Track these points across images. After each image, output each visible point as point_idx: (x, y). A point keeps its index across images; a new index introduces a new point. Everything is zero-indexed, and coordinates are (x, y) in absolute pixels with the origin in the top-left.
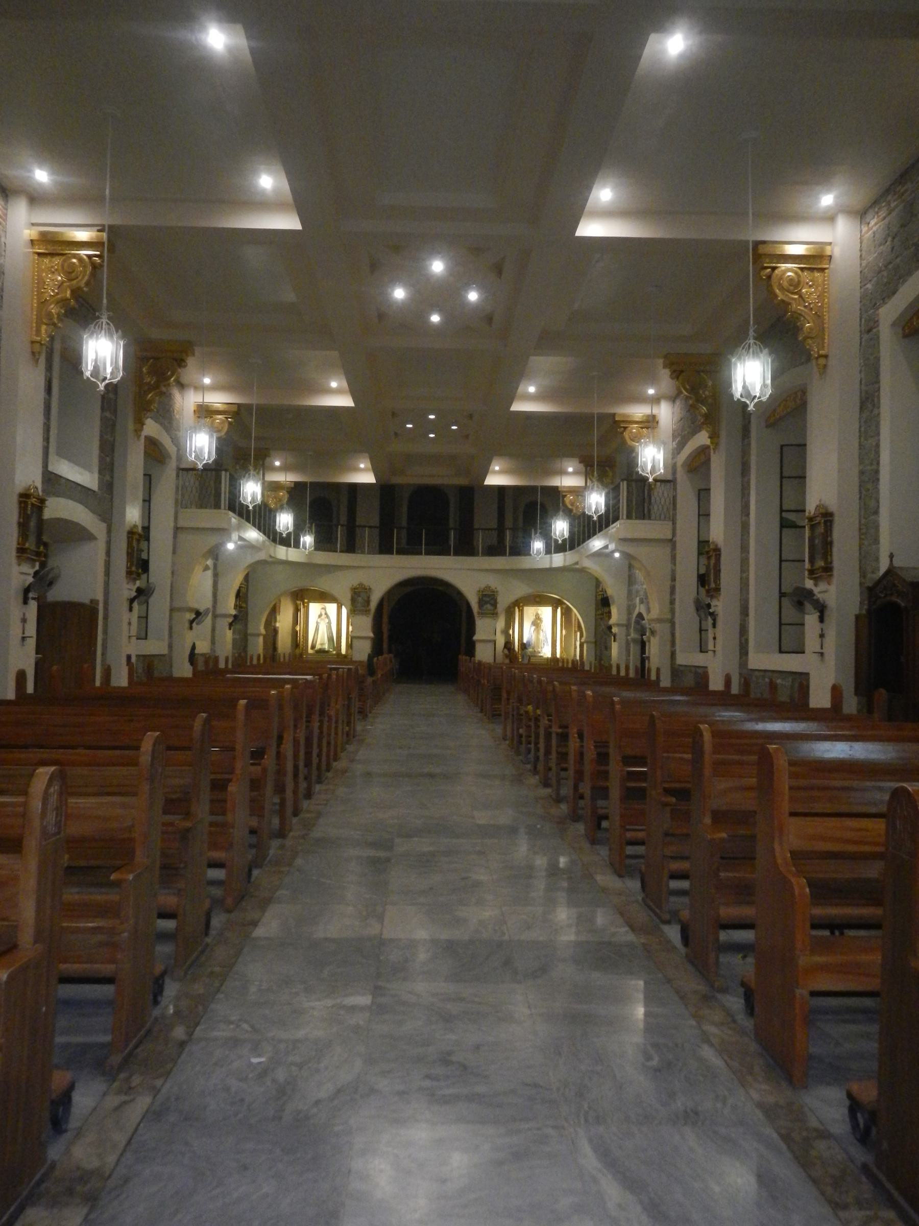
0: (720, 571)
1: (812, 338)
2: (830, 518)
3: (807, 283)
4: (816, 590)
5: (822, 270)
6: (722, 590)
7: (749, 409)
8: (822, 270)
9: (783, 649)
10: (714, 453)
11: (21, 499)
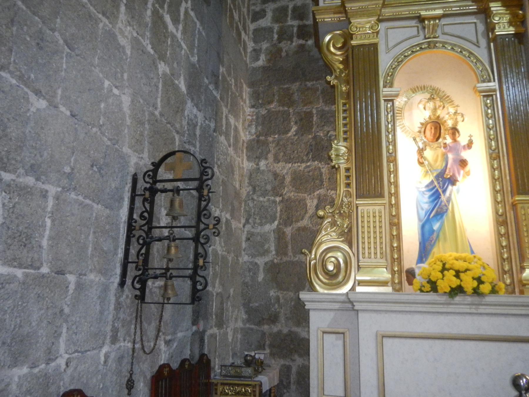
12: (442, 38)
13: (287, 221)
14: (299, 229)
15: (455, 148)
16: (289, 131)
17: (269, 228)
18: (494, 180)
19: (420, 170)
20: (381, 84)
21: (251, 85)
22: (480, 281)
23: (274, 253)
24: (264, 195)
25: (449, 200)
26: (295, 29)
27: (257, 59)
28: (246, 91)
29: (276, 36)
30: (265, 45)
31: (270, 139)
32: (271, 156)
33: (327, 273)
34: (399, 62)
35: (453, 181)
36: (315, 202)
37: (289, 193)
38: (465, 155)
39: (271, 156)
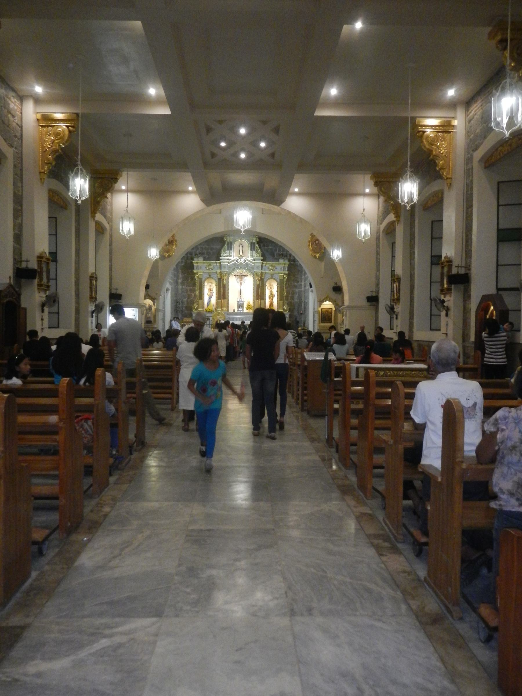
1: (444, 169)
2: (451, 263)
3: (441, 140)
4: (446, 299)
5: (450, 132)
6: (401, 299)
7: (408, 208)
8: (450, 132)
9: (432, 329)
10: (398, 225)
11: (39, 259)
13: (189, 298)
15: (212, 293)
16: (189, 280)
17: (185, 300)
19: (207, 296)
21: (181, 270)
22: (211, 310)
28: (180, 271)
31: (185, 282)
34: (205, 280)
36: (194, 295)
37: (189, 293)
38: (213, 294)
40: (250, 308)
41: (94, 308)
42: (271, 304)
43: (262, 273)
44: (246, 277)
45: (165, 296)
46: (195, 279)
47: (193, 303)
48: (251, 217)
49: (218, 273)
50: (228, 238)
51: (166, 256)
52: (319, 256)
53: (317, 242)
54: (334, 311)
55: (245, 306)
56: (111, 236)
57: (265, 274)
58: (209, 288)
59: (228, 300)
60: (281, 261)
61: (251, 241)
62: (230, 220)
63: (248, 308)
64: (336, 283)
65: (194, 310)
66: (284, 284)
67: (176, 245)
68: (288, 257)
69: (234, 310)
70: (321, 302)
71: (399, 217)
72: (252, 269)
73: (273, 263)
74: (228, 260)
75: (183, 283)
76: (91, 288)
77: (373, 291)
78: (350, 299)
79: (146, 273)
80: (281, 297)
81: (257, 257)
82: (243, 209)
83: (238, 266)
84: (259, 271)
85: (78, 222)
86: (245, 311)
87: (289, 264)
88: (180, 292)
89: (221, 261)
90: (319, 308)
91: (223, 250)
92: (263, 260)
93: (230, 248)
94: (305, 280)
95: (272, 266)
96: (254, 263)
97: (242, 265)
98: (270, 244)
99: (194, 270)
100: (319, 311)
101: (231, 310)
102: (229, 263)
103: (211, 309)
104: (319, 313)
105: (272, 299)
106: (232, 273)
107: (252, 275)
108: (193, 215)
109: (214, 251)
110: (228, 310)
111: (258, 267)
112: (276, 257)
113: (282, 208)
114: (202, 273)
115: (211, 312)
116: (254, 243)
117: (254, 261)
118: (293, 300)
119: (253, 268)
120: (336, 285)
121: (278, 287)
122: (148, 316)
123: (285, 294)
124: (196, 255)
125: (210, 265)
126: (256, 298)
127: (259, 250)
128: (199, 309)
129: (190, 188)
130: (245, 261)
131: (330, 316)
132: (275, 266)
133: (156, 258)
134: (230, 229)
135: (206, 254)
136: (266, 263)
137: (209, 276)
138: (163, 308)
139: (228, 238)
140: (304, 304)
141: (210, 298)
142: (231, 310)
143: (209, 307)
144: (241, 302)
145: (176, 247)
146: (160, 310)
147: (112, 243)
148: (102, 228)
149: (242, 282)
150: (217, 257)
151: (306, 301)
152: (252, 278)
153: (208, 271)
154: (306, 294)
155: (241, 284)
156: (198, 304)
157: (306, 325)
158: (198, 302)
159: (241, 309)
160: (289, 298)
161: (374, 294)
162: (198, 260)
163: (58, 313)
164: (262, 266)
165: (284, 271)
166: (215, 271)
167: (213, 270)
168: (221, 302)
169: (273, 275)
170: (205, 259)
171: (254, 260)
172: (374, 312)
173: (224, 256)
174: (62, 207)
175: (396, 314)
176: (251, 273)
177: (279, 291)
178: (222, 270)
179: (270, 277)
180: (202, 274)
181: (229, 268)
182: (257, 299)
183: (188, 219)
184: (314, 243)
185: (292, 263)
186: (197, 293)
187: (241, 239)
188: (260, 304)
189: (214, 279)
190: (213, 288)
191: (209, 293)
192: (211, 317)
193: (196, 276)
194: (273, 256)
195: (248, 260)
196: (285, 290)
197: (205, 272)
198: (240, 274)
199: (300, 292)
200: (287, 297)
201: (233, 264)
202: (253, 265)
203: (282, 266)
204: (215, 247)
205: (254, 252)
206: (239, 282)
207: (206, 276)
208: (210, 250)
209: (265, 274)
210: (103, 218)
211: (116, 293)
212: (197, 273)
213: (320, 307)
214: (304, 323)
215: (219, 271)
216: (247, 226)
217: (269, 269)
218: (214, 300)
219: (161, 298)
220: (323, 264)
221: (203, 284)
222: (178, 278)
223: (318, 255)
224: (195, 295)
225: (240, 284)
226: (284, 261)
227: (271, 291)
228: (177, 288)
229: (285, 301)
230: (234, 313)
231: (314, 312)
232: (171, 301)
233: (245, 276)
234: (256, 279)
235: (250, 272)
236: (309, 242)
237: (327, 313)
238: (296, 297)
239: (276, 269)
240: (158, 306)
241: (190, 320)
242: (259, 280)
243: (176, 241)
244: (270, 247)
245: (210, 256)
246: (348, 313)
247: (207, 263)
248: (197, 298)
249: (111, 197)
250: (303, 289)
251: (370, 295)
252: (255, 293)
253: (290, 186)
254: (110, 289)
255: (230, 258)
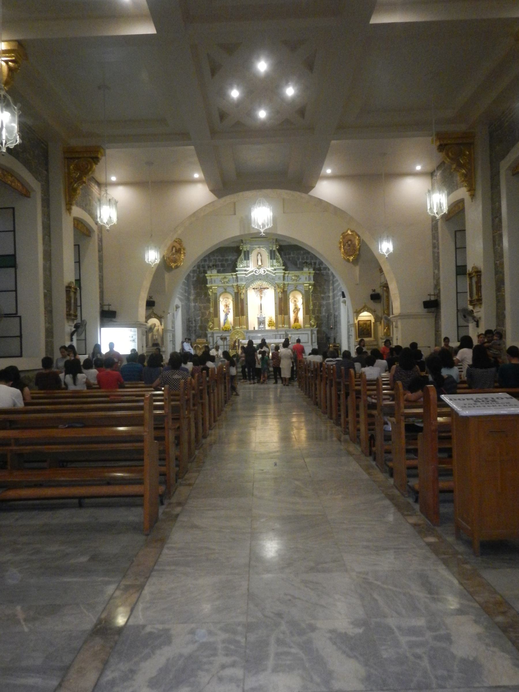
0: (481, 286)
12: (227, 291)
13: (203, 317)
14: (205, 318)
15: (229, 309)
17: (199, 318)
18: (233, 314)
19: (223, 312)
20: (218, 299)
21: (193, 285)
22: (228, 329)
23: (200, 323)
24: (197, 311)
25: (227, 317)
26: (202, 271)
27: (193, 278)
28: (192, 286)
29: (198, 272)
30: (195, 275)
31: (198, 298)
32: (198, 302)
33: (210, 328)
34: (220, 295)
35: (228, 314)
38: (230, 310)
39: (198, 302)
40: (273, 324)
41: (74, 329)
42: (296, 320)
43: (284, 284)
44: (266, 290)
45: (173, 315)
46: (209, 295)
47: (208, 322)
48: (271, 214)
49: (235, 287)
50: (245, 246)
51: (173, 267)
52: (353, 260)
53: (349, 242)
54: (373, 323)
55: (267, 323)
56: (101, 240)
57: (288, 286)
58: (225, 304)
59: (247, 317)
60: (306, 270)
61: (271, 249)
62: (247, 221)
63: (270, 325)
64: (374, 291)
65: (209, 330)
66: (310, 297)
67: (184, 253)
68: (313, 266)
69: (254, 328)
70: (357, 313)
71: (474, 190)
72: (272, 281)
73: (296, 272)
74: (245, 271)
75: (195, 300)
76: (68, 303)
77: (432, 294)
78: (402, 306)
79: (147, 284)
80: (307, 311)
81: (278, 266)
82: (261, 204)
83: (258, 278)
84: (281, 282)
85: (47, 216)
86: (267, 328)
87: (315, 273)
88: (193, 310)
89: (237, 273)
90: (355, 320)
91: (239, 260)
92: (285, 270)
93: (247, 258)
94: (333, 292)
95: (295, 276)
96: (275, 274)
97: (261, 276)
98: (292, 253)
99: (207, 284)
100: (355, 324)
101: (251, 328)
102: (246, 274)
103: (228, 328)
104: (356, 326)
105: (297, 314)
106: (251, 286)
107: (273, 288)
108: (201, 209)
109: (229, 262)
110: (247, 328)
111: (279, 278)
112: (298, 266)
113: (311, 197)
114: (216, 287)
115: (228, 331)
116: (274, 251)
117: (275, 271)
118: (321, 313)
119: (274, 279)
120: (374, 293)
121: (303, 299)
122: (154, 338)
123: (311, 307)
124: (209, 267)
125: (225, 278)
126: (278, 312)
127: (280, 259)
128: (215, 329)
129: (196, 176)
130: (265, 272)
131: (368, 330)
132: (299, 276)
133: (156, 263)
134: (246, 232)
135: (220, 266)
136: (289, 273)
137: (224, 291)
138: (172, 328)
139: (245, 246)
140: (335, 318)
141: (227, 315)
142: (251, 328)
143: (226, 325)
144: (261, 318)
145: (184, 255)
146: (169, 330)
147: (102, 249)
148: (87, 228)
149: (262, 295)
150: (233, 268)
151: (337, 314)
152: (273, 291)
153: (223, 285)
154: (335, 306)
155: (261, 297)
156: (213, 323)
157: (338, 341)
158: (213, 320)
159: (262, 326)
160: (316, 311)
161: (433, 298)
162: (211, 273)
163: (21, 336)
164: (284, 277)
165: (309, 281)
166: (231, 285)
167: (228, 283)
168: (240, 319)
169: (297, 286)
170: (219, 272)
171: (275, 270)
172: (433, 320)
173: (240, 266)
174: (22, 194)
175: (476, 320)
176: (272, 285)
177: (304, 304)
178: (239, 283)
179: (294, 288)
180: (217, 288)
181: (246, 280)
182: (281, 313)
183: (194, 214)
184: (347, 244)
185: (318, 272)
186: (212, 310)
187: (259, 247)
188: (284, 320)
189: (231, 294)
190: (229, 304)
191: (225, 310)
192: (229, 336)
193: (210, 291)
194: (295, 264)
195: (268, 271)
196: (311, 303)
197: (220, 287)
198: (260, 287)
199: (328, 305)
200: (313, 311)
201: (251, 276)
202: (274, 275)
203: (307, 275)
204: (230, 258)
205: (275, 261)
206: (259, 296)
207: (221, 290)
208: (224, 262)
209: (288, 286)
210: (89, 216)
211: (109, 309)
212: (211, 288)
213: (357, 319)
214: (335, 339)
215: (235, 284)
216: (268, 225)
217: (292, 279)
218: (231, 317)
219: (169, 316)
220: (357, 269)
221: (218, 300)
222: (189, 294)
223: (351, 258)
224: (210, 313)
225: (259, 298)
226: (309, 269)
227: (296, 305)
228: (189, 306)
229: (313, 316)
230: (254, 331)
231: (349, 326)
232: (183, 320)
233: (265, 288)
234: (278, 291)
235: (270, 284)
236: (340, 243)
237: (365, 325)
238: (324, 309)
239: (300, 279)
240: (164, 326)
241: (204, 340)
242: (281, 293)
243: (184, 249)
244: (292, 255)
245: (225, 268)
246: (399, 324)
247: (222, 275)
248: (212, 316)
249: (99, 191)
250: (331, 301)
251: (427, 299)
252: (278, 306)
253: (321, 168)
254: (102, 305)
255: (247, 269)
